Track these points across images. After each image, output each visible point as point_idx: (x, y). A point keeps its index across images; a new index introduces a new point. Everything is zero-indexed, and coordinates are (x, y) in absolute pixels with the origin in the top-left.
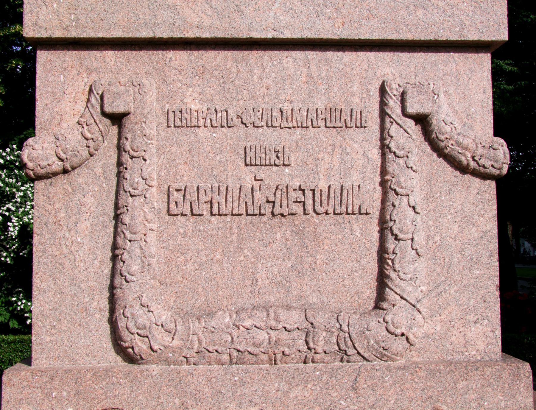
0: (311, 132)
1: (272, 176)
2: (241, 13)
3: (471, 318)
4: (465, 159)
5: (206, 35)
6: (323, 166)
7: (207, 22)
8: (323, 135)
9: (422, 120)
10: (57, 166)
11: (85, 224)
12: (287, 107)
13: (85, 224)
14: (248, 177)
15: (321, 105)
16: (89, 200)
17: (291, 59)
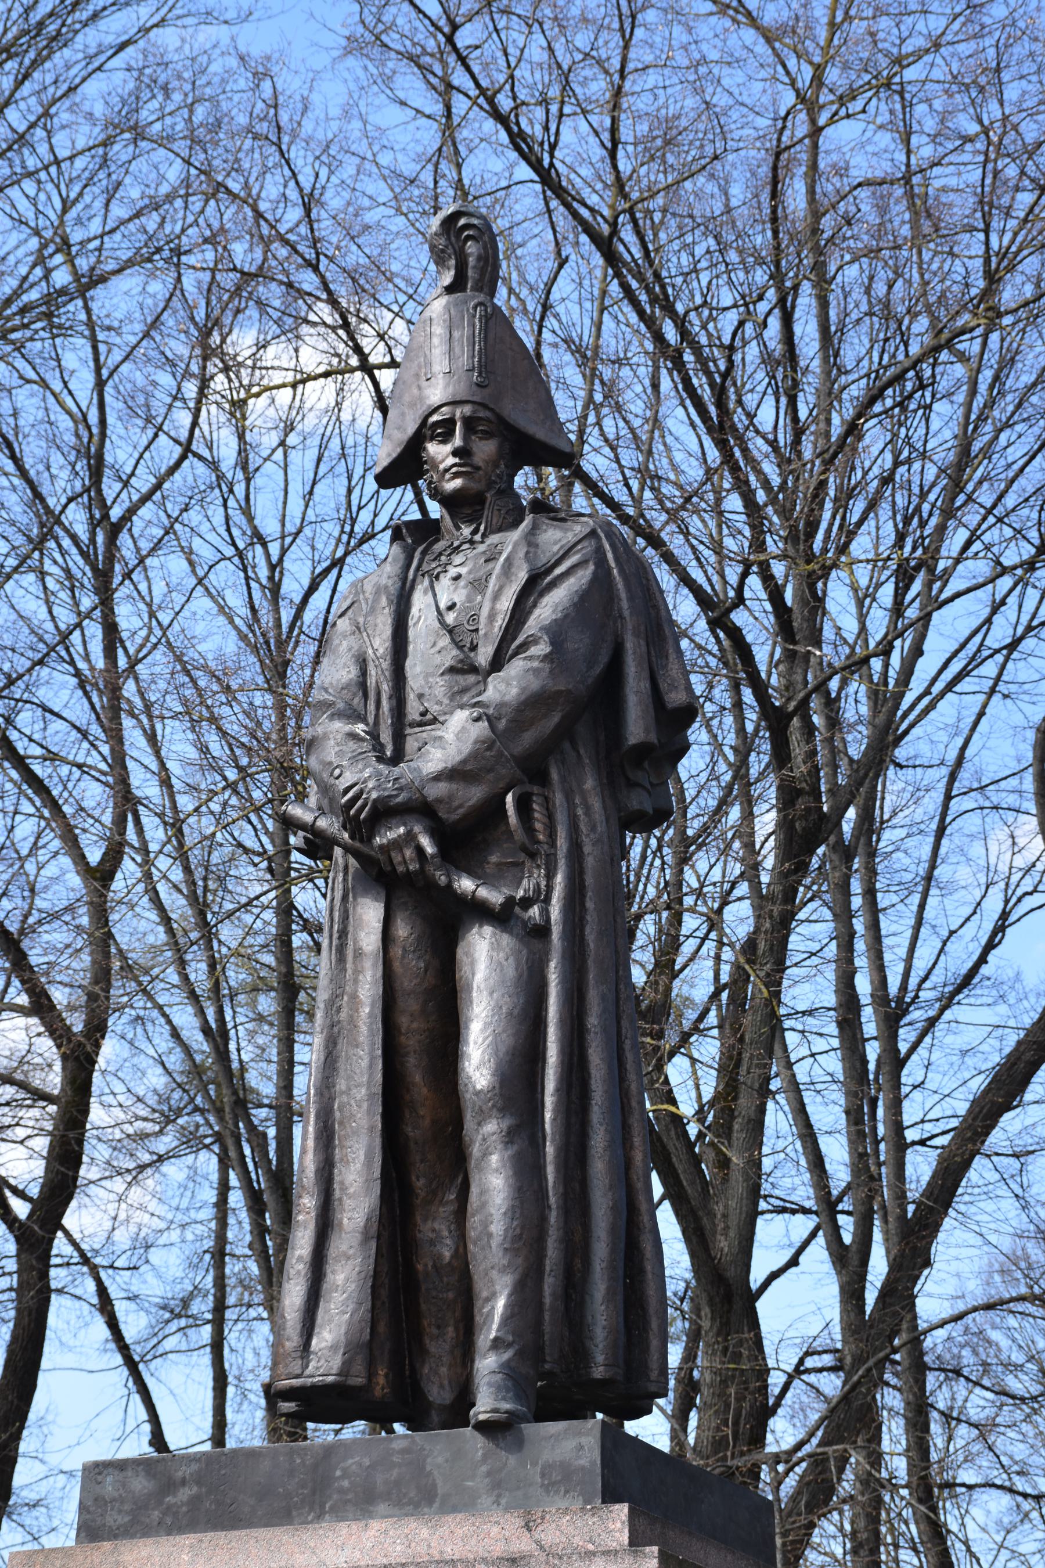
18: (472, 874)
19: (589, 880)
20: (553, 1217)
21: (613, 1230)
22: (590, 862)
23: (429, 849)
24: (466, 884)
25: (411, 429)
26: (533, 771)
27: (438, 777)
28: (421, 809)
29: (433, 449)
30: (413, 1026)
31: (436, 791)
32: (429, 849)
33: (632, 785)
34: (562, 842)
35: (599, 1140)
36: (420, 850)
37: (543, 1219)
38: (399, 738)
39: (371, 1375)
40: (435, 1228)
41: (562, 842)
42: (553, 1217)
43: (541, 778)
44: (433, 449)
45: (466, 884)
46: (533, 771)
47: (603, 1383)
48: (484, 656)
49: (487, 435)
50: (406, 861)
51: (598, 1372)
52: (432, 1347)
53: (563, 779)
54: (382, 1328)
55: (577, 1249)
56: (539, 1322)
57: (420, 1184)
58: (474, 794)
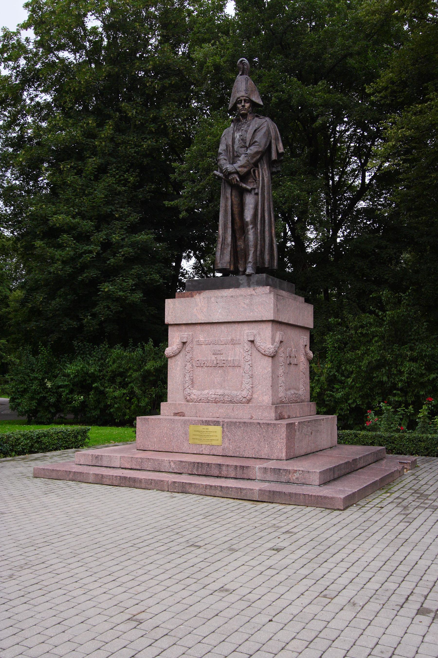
0: (227, 345)
1: (219, 357)
2: (211, 316)
3: (264, 394)
4: (263, 352)
5: (203, 322)
6: (230, 354)
7: (203, 318)
8: (230, 346)
9: (252, 342)
10: (172, 355)
11: (178, 369)
12: (222, 339)
13: (178, 369)
14: (213, 357)
15: (230, 339)
16: (179, 363)
17: (223, 327)
18: (245, 184)
19: (265, 184)
20: (259, 242)
21: (269, 244)
22: (266, 181)
23: (238, 180)
24: (244, 185)
25: (235, 101)
26: (256, 165)
27: (239, 167)
28: (237, 173)
29: (239, 106)
30: (236, 210)
31: (239, 169)
32: (238, 180)
33: (273, 167)
34: (261, 178)
35: (267, 228)
36: (237, 180)
37: (257, 242)
38: (233, 159)
39: (230, 266)
40: (240, 243)
41: (261, 178)
42: (259, 242)
43: (257, 167)
44: (239, 106)
45: (244, 185)
46: (256, 165)
47: (268, 268)
48: (247, 144)
49: (248, 103)
50: (234, 182)
51: (266, 266)
52: (240, 262)
53: (261, 166)
54: (232, 259)
55: (263, 247)
56: (256, 259)
57: (238, 236)
58: (245, 170)
